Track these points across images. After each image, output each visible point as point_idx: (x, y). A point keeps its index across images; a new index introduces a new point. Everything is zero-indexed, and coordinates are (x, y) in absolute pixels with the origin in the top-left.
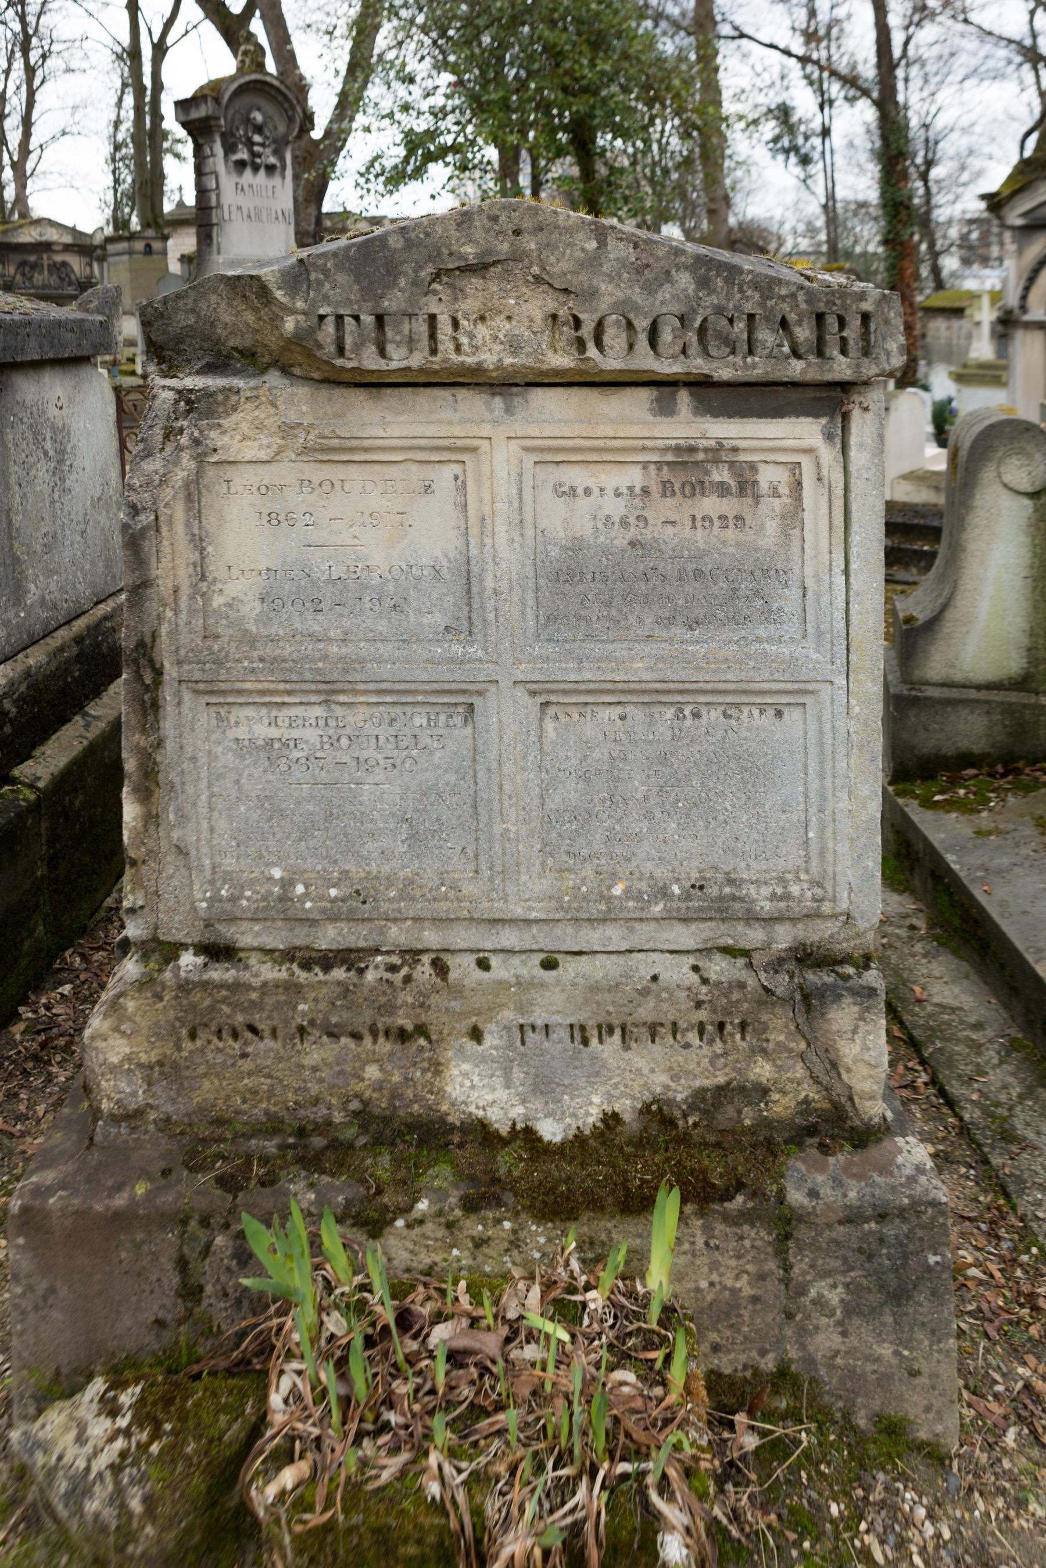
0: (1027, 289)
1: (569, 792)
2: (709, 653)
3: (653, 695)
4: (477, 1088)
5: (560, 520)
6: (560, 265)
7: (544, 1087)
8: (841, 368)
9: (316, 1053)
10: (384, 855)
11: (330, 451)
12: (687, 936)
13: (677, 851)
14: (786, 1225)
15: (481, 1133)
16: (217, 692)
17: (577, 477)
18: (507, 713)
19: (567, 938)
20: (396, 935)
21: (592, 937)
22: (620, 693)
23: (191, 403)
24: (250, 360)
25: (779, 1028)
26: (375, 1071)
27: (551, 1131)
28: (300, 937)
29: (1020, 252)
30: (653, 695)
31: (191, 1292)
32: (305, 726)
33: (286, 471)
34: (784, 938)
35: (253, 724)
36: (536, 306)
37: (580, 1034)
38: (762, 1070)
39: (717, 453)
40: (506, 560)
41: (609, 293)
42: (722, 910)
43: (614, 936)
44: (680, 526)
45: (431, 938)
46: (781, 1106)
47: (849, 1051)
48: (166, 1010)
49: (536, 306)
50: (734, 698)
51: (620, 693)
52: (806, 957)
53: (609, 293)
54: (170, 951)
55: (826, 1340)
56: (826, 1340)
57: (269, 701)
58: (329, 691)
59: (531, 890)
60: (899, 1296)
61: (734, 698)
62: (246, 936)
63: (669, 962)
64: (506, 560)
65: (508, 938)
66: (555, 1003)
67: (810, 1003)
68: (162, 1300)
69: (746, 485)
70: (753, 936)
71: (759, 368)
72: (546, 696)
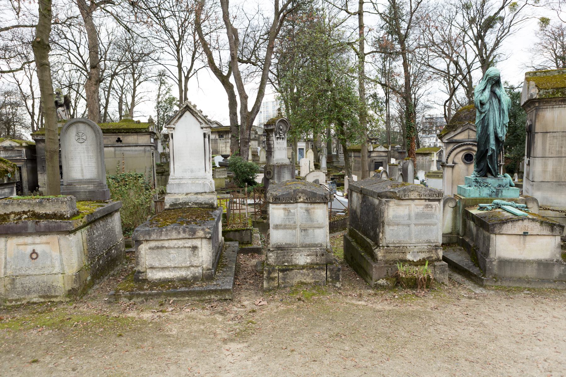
0: (448, 158)
1: (417, 233)
2: (428, 221)
3: (424, 225)
4: (409, 257)
5: (417, 211)
6: (419, 190)
7: (415, 257)
8: (440, 198)
9: (396, 254)
10: (402, 238)
11: (398, 205)
12: (426, 244)
13: (425, 238)
14: (435, 266)
15: (409, 261)
16: (389, 225)
17: (418, 207)
18: (412, 226)
19: (416, 245)
20: (403, 245)
21: (419, 245)
22: (421, 224)
23: (387, 201)
24: (391, 198)
25: (434, 251)
26: (401, 256)
27: (415, 261)
28: (395, 245)
29: (446, 148)
30: (424, 225)
31: (388, 273)
32: (395, 228)
33: (395, 207)
34: (434, 244)
35: (391, 228)
36: (417, 193)
37: (418, 252)
38: (432, 255)
39: (430, 205)
40: (413, 214)
41: (423, 192)
42: (429, 242)
43: (420, 245)
44: (427, 211)
45: (405, 245)
46: (434, 258)
47: (439, 253)
48: (384, 251)
49: (417, 193)
50: (430, 225)
51: (421, 224)
52: (436, 246)
53: (423, 192)
54: (384, 247)
55: (438, 276)
56: (438, 276)
57: (393, 226)
58: (398, 225)
59: (414, 241)
60: (444, 272)
61: (430, 225)
62: (390, 245)
63: (425, 246)
64: (413, 214)
65: (412, 245)
66: (416, 250)
67: (436, 249)
68: (385, 273)
69: (432, 207)
70: (431, 244)
71: (434, 198)
72: (415, 225)
